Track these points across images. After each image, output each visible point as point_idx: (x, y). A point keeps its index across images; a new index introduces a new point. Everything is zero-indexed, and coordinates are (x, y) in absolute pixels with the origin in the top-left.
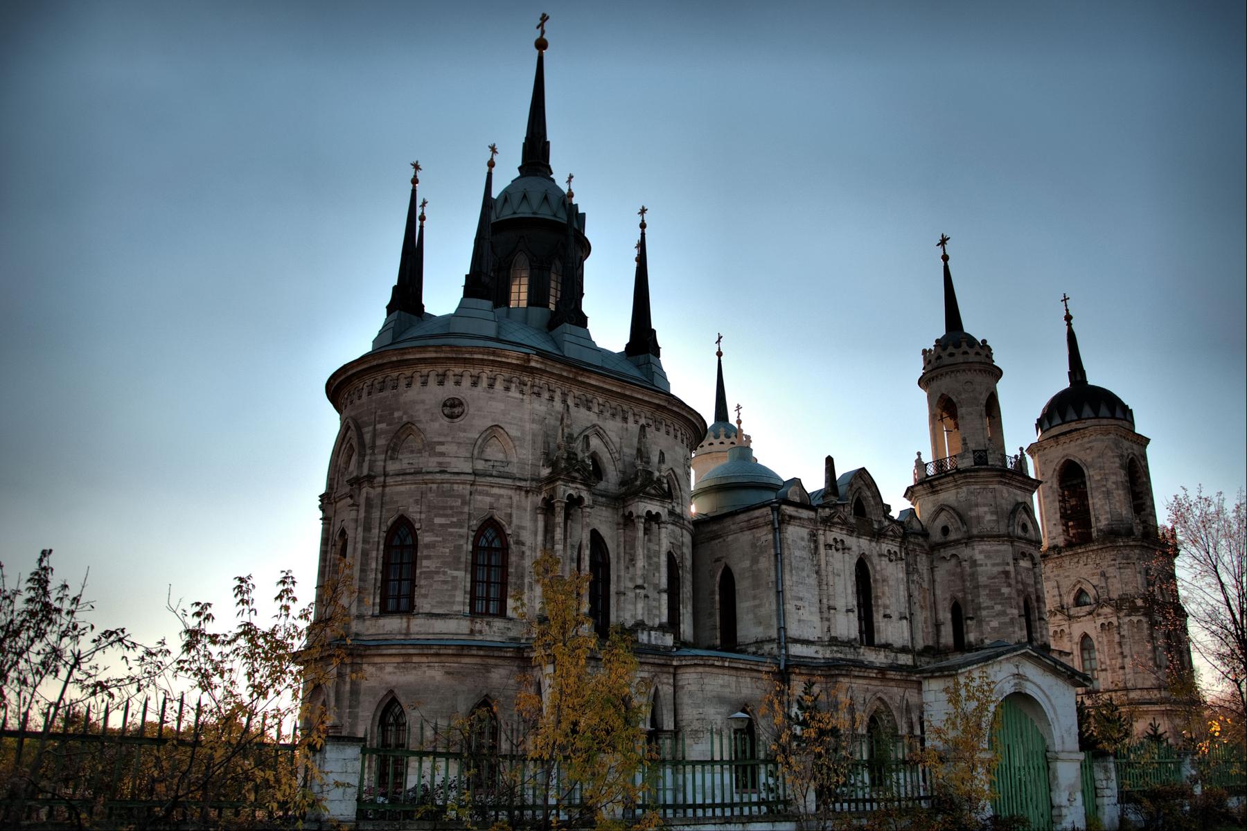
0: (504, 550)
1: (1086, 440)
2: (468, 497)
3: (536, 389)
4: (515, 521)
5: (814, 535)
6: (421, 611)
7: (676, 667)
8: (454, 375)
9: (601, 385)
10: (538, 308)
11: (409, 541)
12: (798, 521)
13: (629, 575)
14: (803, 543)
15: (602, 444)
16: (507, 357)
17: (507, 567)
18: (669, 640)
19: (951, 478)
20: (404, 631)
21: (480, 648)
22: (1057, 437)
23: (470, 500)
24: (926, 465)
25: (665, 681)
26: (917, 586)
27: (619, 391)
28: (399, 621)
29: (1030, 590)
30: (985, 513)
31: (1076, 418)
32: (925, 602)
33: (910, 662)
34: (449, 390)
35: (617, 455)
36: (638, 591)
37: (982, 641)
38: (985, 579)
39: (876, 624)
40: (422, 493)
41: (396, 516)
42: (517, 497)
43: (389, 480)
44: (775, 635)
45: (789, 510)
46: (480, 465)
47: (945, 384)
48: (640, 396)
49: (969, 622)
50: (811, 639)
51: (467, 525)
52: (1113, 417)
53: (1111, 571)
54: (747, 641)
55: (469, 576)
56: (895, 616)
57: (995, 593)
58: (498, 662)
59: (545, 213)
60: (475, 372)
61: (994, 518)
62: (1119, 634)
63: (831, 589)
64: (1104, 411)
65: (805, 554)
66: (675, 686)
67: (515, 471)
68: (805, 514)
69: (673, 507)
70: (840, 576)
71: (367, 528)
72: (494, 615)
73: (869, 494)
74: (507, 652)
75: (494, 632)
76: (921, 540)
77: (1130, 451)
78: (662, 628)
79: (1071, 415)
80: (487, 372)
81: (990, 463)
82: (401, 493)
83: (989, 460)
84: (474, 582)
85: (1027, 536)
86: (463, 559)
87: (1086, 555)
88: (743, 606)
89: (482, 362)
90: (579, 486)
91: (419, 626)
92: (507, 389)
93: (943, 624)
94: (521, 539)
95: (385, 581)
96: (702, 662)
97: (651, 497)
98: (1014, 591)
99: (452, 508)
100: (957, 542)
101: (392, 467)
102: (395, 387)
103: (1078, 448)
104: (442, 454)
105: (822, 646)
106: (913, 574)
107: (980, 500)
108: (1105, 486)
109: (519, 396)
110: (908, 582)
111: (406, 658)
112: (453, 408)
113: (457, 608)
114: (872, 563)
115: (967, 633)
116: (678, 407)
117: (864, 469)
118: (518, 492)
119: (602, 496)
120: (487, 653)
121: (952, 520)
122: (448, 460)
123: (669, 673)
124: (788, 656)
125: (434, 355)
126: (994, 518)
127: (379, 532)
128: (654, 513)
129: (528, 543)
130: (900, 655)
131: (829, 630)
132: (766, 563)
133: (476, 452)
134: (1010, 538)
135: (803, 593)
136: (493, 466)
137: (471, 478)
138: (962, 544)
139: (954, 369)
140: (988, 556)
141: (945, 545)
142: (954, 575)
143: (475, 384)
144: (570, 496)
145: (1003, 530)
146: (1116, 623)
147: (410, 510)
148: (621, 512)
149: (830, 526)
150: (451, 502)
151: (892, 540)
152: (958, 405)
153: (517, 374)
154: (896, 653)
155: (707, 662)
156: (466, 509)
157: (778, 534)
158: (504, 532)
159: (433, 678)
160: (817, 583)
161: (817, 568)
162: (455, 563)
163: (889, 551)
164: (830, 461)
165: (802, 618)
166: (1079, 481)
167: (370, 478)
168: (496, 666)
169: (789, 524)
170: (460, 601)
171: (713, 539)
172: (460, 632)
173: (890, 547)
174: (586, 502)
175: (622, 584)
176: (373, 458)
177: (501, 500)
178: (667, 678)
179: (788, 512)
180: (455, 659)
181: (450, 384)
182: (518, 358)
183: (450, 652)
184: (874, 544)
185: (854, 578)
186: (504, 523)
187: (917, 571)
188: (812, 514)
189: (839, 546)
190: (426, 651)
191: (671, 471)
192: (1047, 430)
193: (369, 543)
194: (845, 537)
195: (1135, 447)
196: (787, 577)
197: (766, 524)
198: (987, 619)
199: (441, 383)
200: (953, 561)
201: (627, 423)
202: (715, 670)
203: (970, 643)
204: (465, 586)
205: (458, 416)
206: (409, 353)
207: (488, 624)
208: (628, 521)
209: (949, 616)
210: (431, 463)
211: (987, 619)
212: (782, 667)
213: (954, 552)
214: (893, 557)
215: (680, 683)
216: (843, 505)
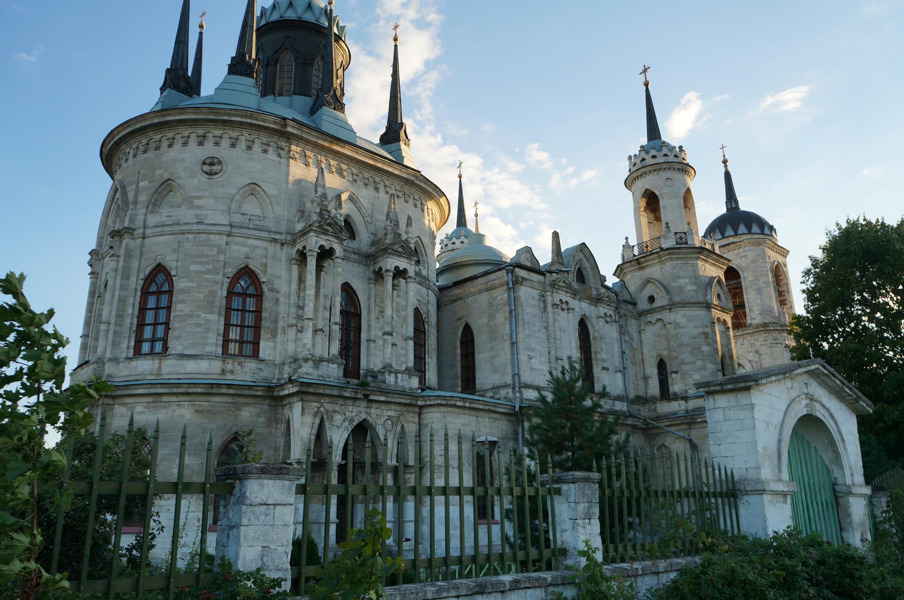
1: (741, 250)
2: (224, 247)
4: (270, 269)
6: (173, 352)
7: (421, 407)
8: (214, 137)
9: (355, 155)
10: (302, 97)
11: (166, 287)
12: (529, 282)
14: (534, 302)
15: (355, 209)
17: (261, 312)
18: (415, 382)
20: (155, 372)
21: (229, 386)
23: (226, 249)
24: (633, 246)
25: (411, 419)
27: (371, 162)
28: (151, 362)
30: (686, 284)
31: (733, 234)
33: (625, 408)
34: (209, 150)
35: (369, 219)
36: (386, 337)
37: (686, 391)
39: (596, 375)
40: (179, 243)
41: (154, 265)
42: (272, 248)
43: (148, 231)
44: (510, 381)
45: (522, 273)
46: (237, 219)
47: (649, 182)
48: (390, 169)
49: (674, 375)
51: (222, 272)
52: (762, 233)
53: (763, 350)
54: (485, 388)
55: (222, 320)
56: (612, 369)
57: (696, 350)
58: (249, 400)
60: (234, 134)
61: (694, 288)
63: (558, 342)
64: (755, 229)
65: (536, 311)
66: (420, 425)
68: (536, 277)
69: (420, 269)
71: (126, 276)
73: (588, 265)
74: (257, 391)
75: (246, 372)
76: (630, 307)
78: (408, 371)
79: (729, 232)
80: (245, 136)
81: (689, 243)
84: (227, 325)
86: (217, 304)
88: (481, 357)
90: (330, 238)
93: (650, 377)
94: (275, 287)
95: (141, 325)
96: (444, 402)
97: (399, 254)
99: (207, 256)
100: (662, 308)
101: (152, 220)
102: (157, 148)
103: (735, 257)
104: (200, 207)
108: (756, 285)
111: (156, 398)
112: (211, 166)
113: (209, 349)
114: (591, 323)
115: (672, 384)
116: (425, 183)
117: (584, 244)
118: (273, 244)
119: (354, 253)
120: (237, 392)
121: (658, 290)
122: (205, 212)
123: (414, 412)
124: (522, 399)
125: (194, 117)
126: (694, 288)
127: (137, 280)
129: (283, 291)
130: (616, 403)
132: (501, 318)
133: (233, 207)
136: (250, 219)
137: (228, 229)
138: (666, 309)
139: (657, 168)
140: (689, 319)
141: (650, 311)
142: (659, 336)
143: (233, 145)
144: (321, 247)
145: (701, 299)
147: (168, 258)
148: (372, 268)
152: (660, 198)
153: (275, 139)
154: (614, 400)
155: (449, 402)
156: (222, 258)
157: (512, 293)
159: (182, 416)
160: (546, 337)
161: (546, 324)
162: (209, 306)
163: (605, 313)
164: (556, 235)
166: (736, 281)
167: (130, 231)
168: (247, 404)
169: (522, 285)
170: (213, 344)
171: (455, 301)
172: (211, 372)
173: (606, 311)
175: (373, 333)
176: (134, 213)
177: (257, 251)
178: (412, 417)
180: (205, 398)
181: (209, 144)
182: (275, 123)
183: (199, 390)
184: (593, 307)
186: (258, 271)
188: (541, 278)
189: (564, 306)
190: (175, 390)
191: (418, 239)
193: (127, 290)
194: (570, 300)
195: (779, 256)
196: (520, 330)
197: (502, 285)
198: (690, 373)
199: (201, 144)
200: (659, 325)
201: (378, 192)
202: (456, 410)
203: (675, 394)
204: (218, 329)
205: (216, 174)
206: (170, 115)
207: (240, 364)
208: (379, 275)
209: (656, 371)
210: (187, 215)
211: (690, 373)
212: (517, 409)
213: (659, 317)
214: (608, 319)
215: (425, 422)
216: (568, 272)
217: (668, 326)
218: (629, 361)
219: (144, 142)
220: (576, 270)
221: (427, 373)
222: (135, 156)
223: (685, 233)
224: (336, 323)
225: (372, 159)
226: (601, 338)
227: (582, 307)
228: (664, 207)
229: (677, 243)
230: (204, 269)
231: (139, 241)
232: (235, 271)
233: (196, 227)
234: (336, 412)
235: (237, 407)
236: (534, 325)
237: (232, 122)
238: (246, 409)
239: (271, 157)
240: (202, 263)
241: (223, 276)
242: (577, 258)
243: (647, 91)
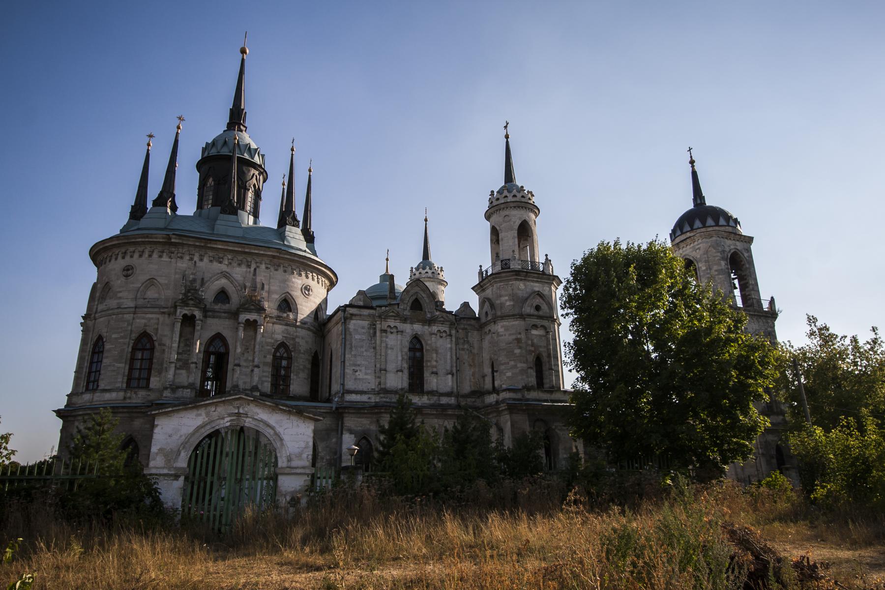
0: (152, 349)
3: (179, 255)
4: (159, 331)
5: (374, 325)
9: (226, 247)
13: (244, 358)
14: (363, 331)
15: (229, 282)
16: (156, 238)
21: (123, 407)
22: (678, 244)
23: (132, 323)
26: (467, 352)
27: (240, 249)
28: (89, 395)
29: (541, 349)
30: (506, 301)
32: (473, 362)
38: (504, 344)
39: (425, 379)
42: (161, 318)
46: (140, 302)
50: (365, 390)
51: (129, 337)
52: (717, 225)
59: (225, 151)
60: (141, 249)
64: (710, 222)
67: (162, 303)
68: (366, 312)
70: (393, 349)
72: (142, 388)
76: (473, 322)
77: (732, 247)
79: (687, 228)
83: (511, 265)
84: (131, 369)
85: (541, 313)
89: (143, 243)
90: (192, 308)
92: (160, 256)
93: (486, 375)
94: (163, 342)
95: (90, 373)
97: (250, 311)
98: (524, 351)
103: (691, 250)
104: (120, 298)
105: (375, 394)
106: (463, 344)
107: (503, 293)
109: (168, 259)
110: (456, 350)
112: (128, 271)
113: (119, 385)
114: (424, 339)
119: (225, 313)
125: (117, 242)
128: (252, 320)
131: (380, 384)
134: (522, 316)
135: (359, 361)
138: (492, 322)
140: (507, 329)
143: (141, 256)
144: (185, 316)
145: (516, 311)
149: (384, 318)
151: (442, 324)
152: (500, 232)
154: (439, 396)
158: (152, 339)
161: (374, 345)
165: (358, 377)
169: (352, 319)
170: (121, 382)
174: (197, 317)
179: (351, 312)
181: (128, 258)
182: (163, 238)
184: (426, 327)
187: (468, 342)
188: (372, 311)
192: (674, 240)
196: (347, 352)
198: (504, 371)
199: (123, 258)
201: (250, 268)
204: (124, 373)
205: (130, 276)
207: (135, 393)
209: (490, 370)
211: (504, 371)
212: (334, 409)
213: (489, 328)
217: (493, 335)
218: (466, 364)
220: (411, 301)
221: (291, 386)
223: (509, 260)
225: (240, 247)
227: (410, 329)
228: (502, 239)
229: (502, 269)
231: (93, 321)
232: (137, 335)
233: (116, 311)
236: (362, 347)
237: (138, 242)
239: (165, 260)
242: (412, 292)
243: (507, 142)
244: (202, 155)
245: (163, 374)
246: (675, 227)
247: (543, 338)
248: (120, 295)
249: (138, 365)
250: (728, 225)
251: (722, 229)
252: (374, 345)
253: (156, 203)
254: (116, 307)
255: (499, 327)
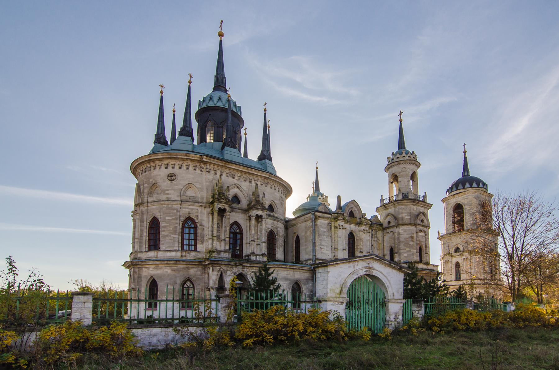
0: (196, 228)
2: (179, 209)
4: (199, 217)
19: (392, 204)
40: (161, 208)
41: (152, 217)
52: (478, 187)
55: (180, 237)
62: (470, 261)
63: (336, 242)
64: (474, 185)
65: (325, 230)
70: (341, 238)
82: (153, 209)
84: (183, 239)
87: (460, 235)
91: (161, 254)
100: (393, 226)
101: (150, 199)
102: (150, 170)
114: (356, 234)
135: (323, 243)
141: (388, 228)
146: (469, 258)
150: (172, 211)
156: (178, 214)
157: (314, 223)
162: (175, 232)
176: (143, 197)
184: (357, 227)
185: (347, 239)
186: (195, 218)
213: (392, 230)
214: (366, 232)
219: (145, 168)
222: (142, 174)
224: (227, 238)
226: (360, 240)
230: (171, 218)
232: (184, 219)
234: (228, 270)
235: (188, 268)
236: (324, 235)
238: (192, 269)
240: (170, 216)
241: (180, 221)
244: (199, 108)
245: (205, 243)
246: (452, 186)
247: (424, 237)
248: (167, 192)
249: (186, 236)
250: (484, 188)
251: (481, 189)
252: (331, 235)
253: (181, 134)
254: (166, 200)
255: (401, 229)
